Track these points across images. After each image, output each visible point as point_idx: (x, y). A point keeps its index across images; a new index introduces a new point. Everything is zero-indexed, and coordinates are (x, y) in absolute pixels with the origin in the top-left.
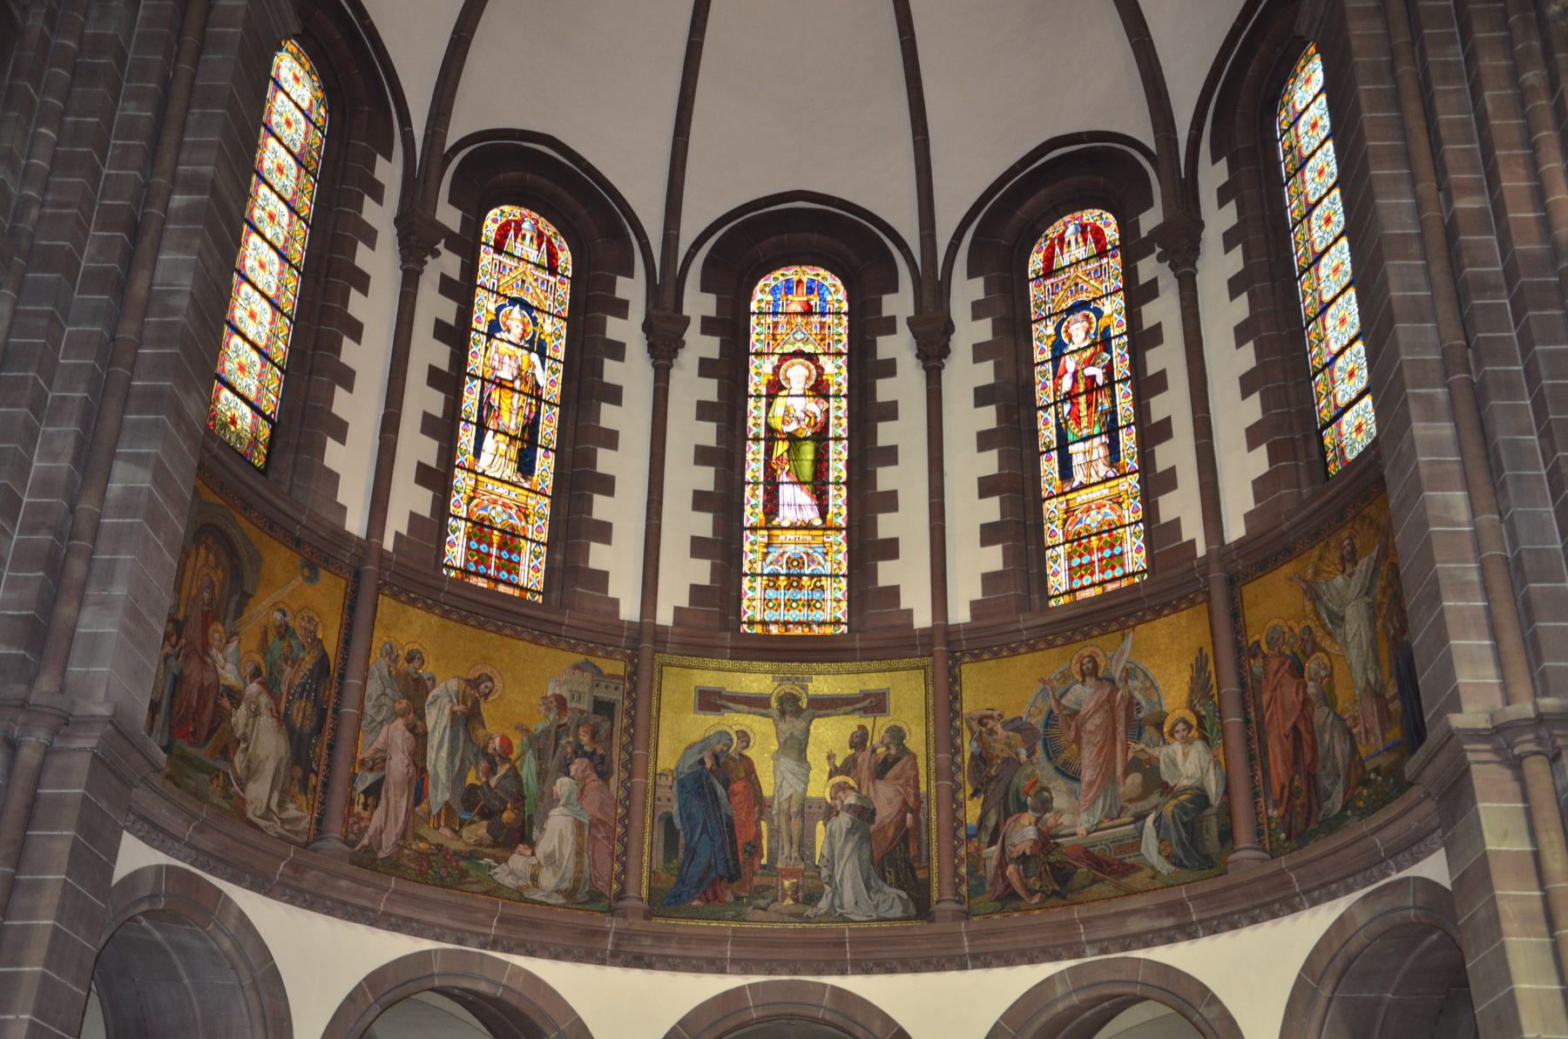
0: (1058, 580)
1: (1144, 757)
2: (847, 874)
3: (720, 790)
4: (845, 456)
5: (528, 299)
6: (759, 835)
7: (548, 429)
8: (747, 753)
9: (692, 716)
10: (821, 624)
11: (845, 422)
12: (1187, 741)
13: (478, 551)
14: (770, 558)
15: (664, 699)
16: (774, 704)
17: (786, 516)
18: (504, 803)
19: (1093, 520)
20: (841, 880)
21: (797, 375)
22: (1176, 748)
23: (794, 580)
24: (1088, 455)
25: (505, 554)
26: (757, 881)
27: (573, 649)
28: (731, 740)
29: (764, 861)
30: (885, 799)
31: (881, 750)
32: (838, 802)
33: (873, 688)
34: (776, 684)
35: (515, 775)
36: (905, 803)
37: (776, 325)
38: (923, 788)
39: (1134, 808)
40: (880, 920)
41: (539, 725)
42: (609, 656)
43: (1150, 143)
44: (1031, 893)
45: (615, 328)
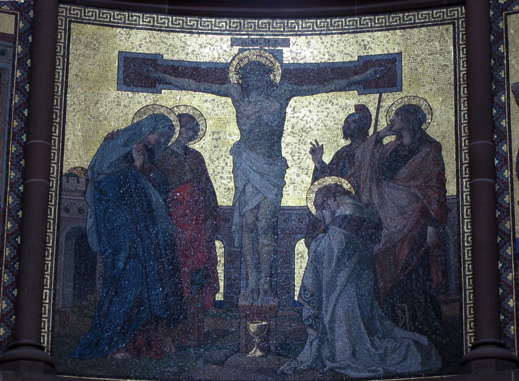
2: (340, 312)
8: (196, 146)
9: (114, 93)
16: (233, 78)
20: (332, 321)
26: (208, 324)
28: (172, 128)
29: (219, 297)
32: (327, 213)
33: (379, 52)
34: (236, 49)
36: (424, 212)
38: (451, 189)
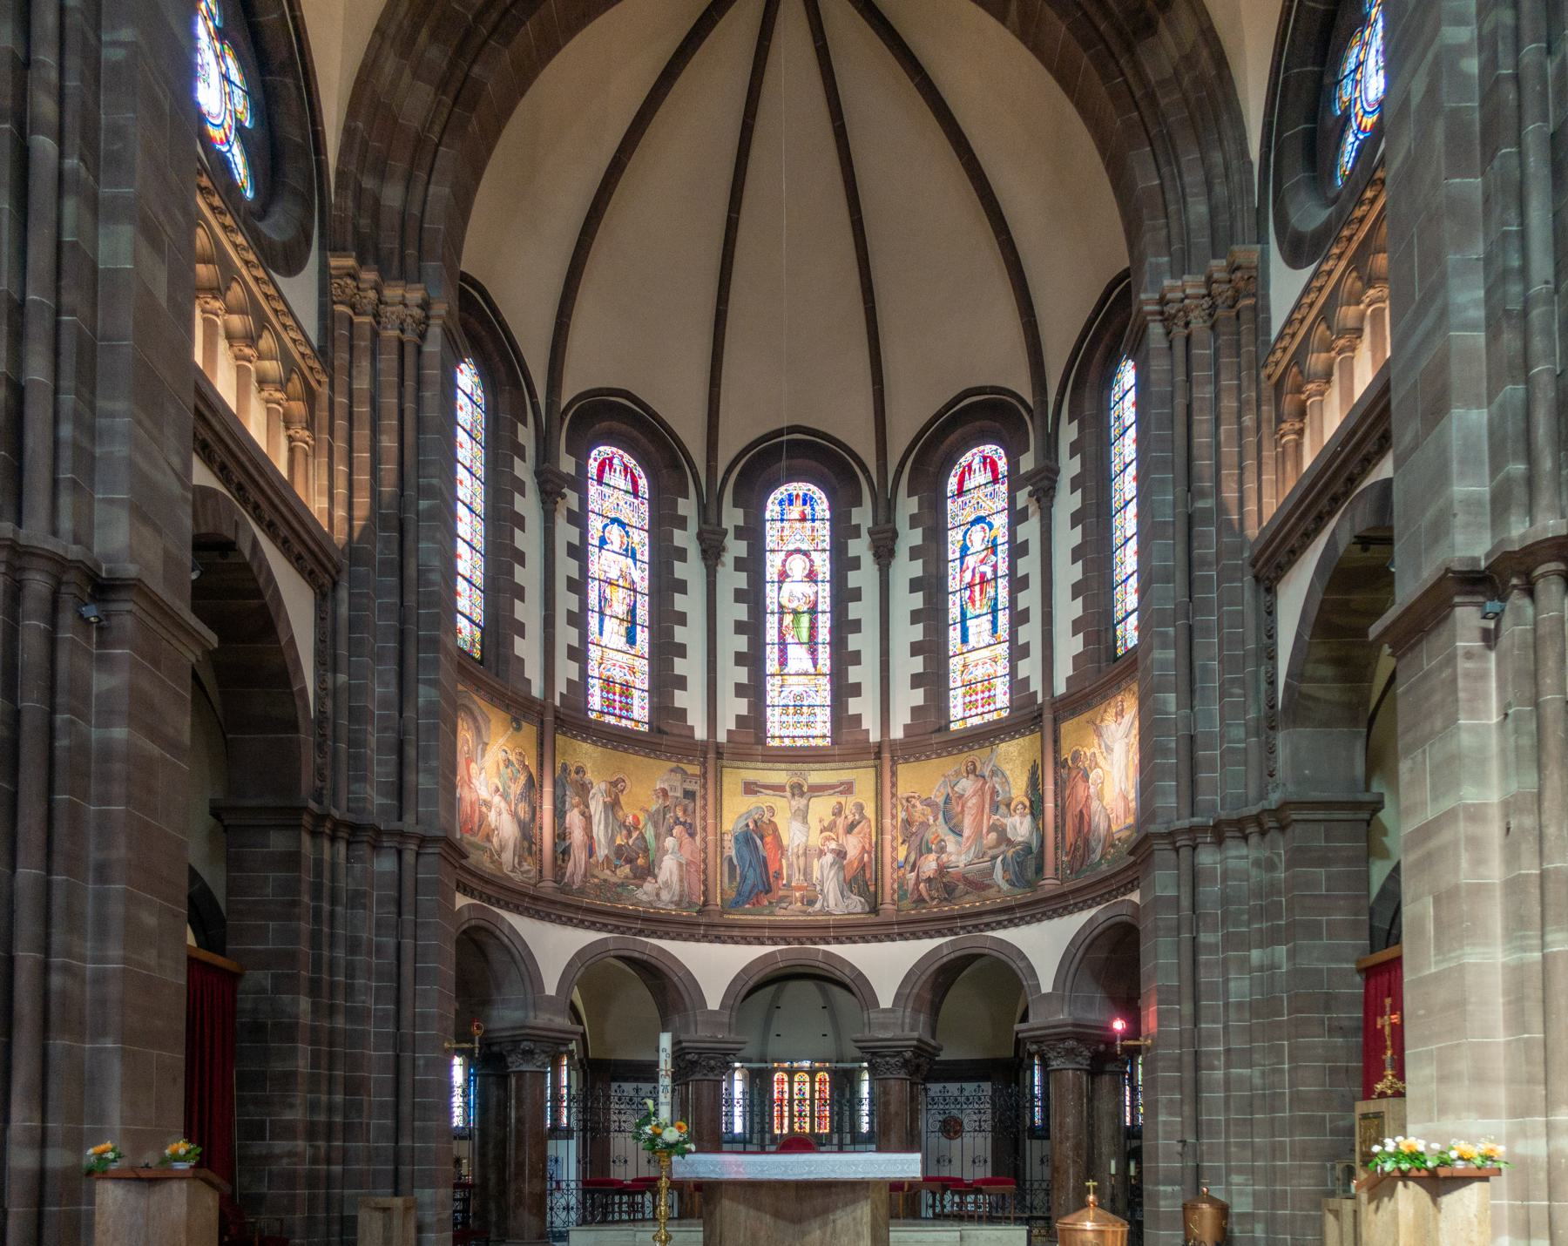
0: (956, 709)
1: (998, 823)
3: (758, 841)
4: (828, 624)
5: (622, 518)
6: (781, 867)
7: (643, 614)
10: (814, 737)
11: (828, 600)
12: (1023, 815)
13: (608, 699)
14: (783, 695)
15: (724, 788)
16: (788, 789)
17: (792, 666)
18: (637, 854)
19: (979, 673)
21: (798, 566)
22: (1017, 819)
23: (798, 708)
24: (979, 629)
25: (624, 700)
26: (781, 893)
27: (669, 759)
30: (853, 845)
31: (851, 818)
35: (642, 837)
36: (864, 847)
37: (783, 529)
39: (995, 851)
40: (849, 914)
41: (654, 807)
42: (690, 762)
43: (1030, 400)
44: (933, 899)
45: (681, 538)
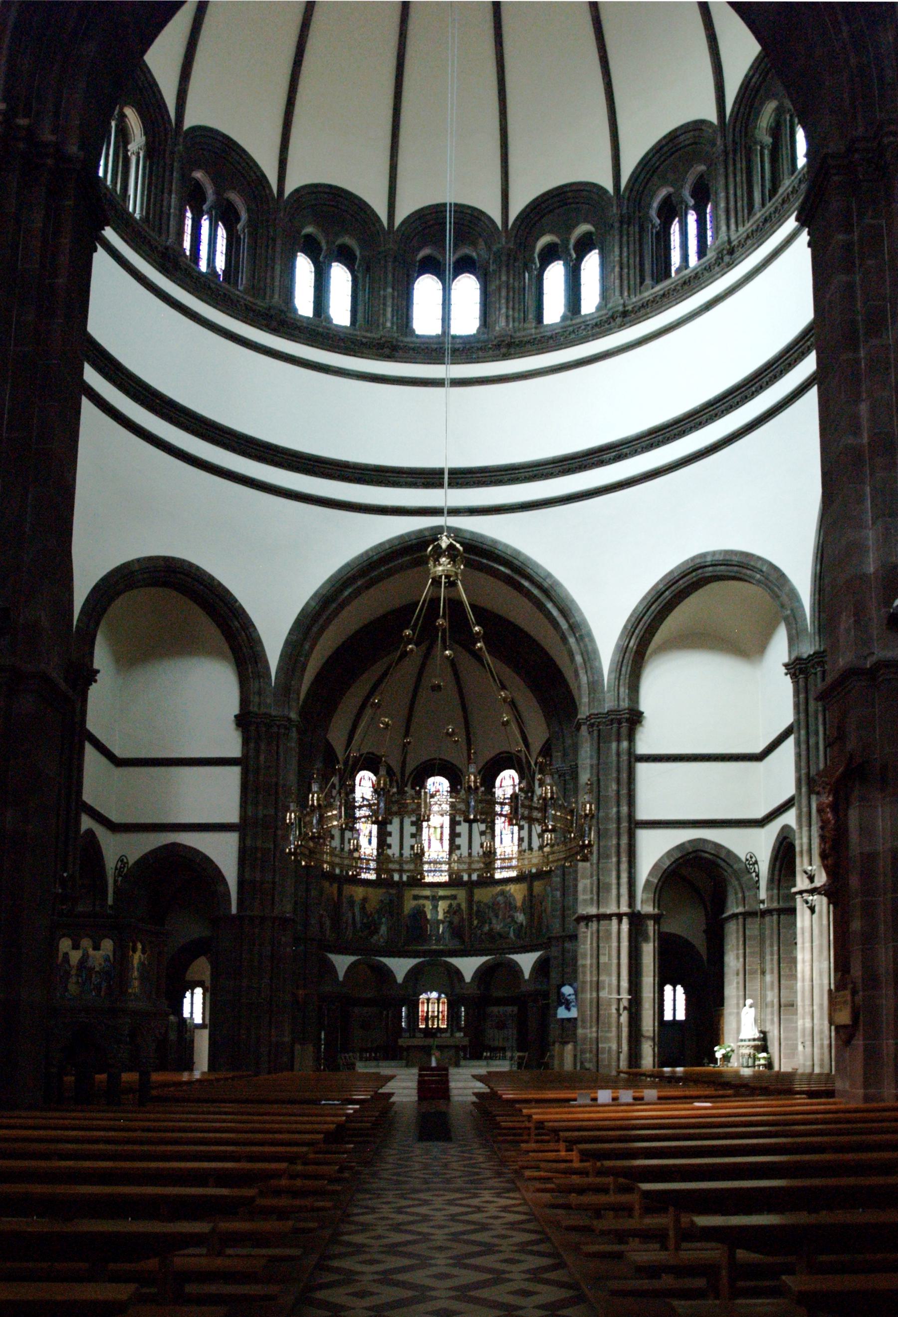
30: (456, 920)
41: (378, 907)
